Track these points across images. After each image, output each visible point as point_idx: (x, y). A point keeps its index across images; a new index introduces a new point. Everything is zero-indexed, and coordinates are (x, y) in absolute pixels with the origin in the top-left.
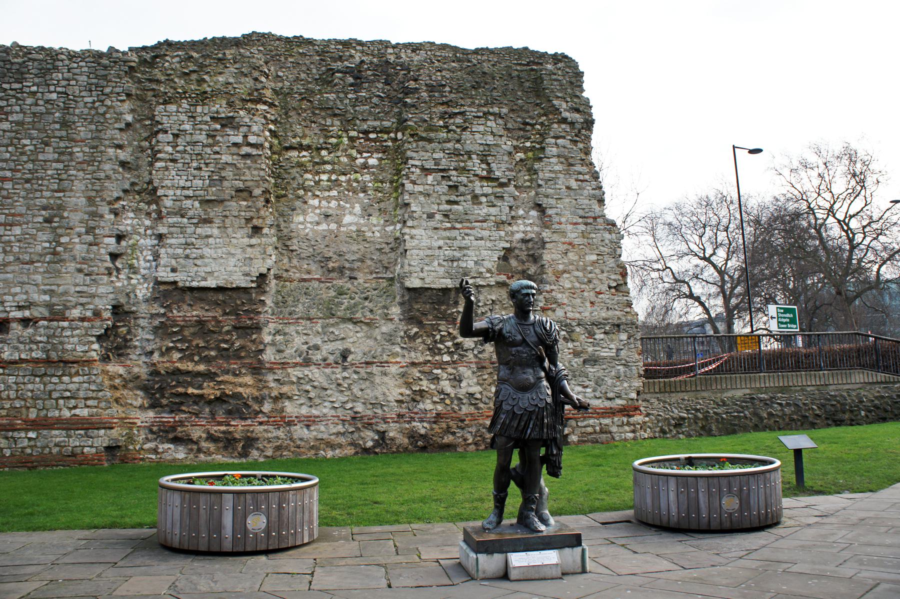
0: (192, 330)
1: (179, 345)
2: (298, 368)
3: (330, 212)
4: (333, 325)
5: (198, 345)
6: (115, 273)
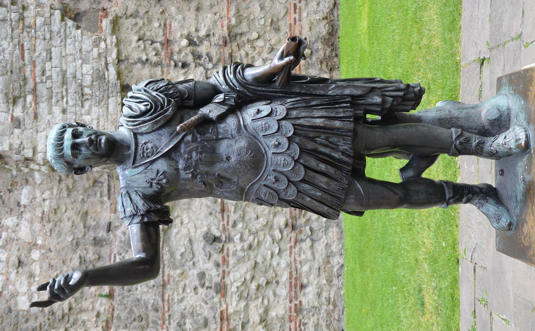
3: (14, 259)
4: (172, 254)
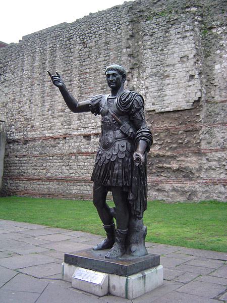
0: (164, 134)
1: (158, 142)
2: (219, 152)
5: (167, 141)
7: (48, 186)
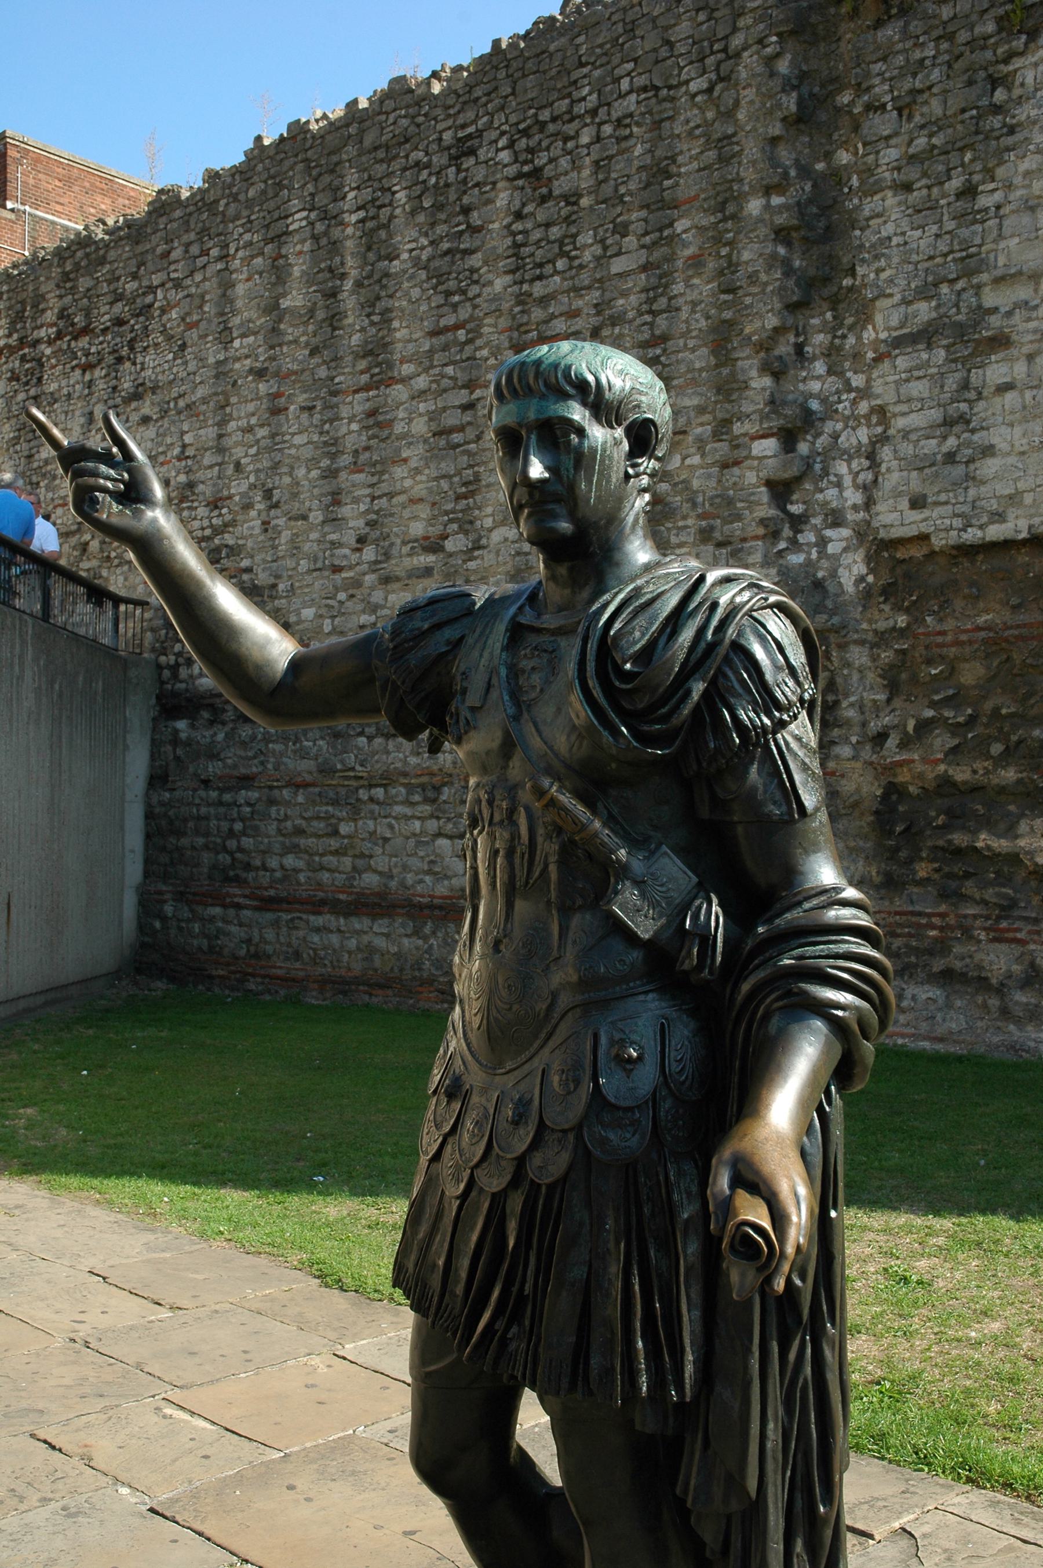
1: (948, 713)
6: (787, 532)
7: (365, 939)
